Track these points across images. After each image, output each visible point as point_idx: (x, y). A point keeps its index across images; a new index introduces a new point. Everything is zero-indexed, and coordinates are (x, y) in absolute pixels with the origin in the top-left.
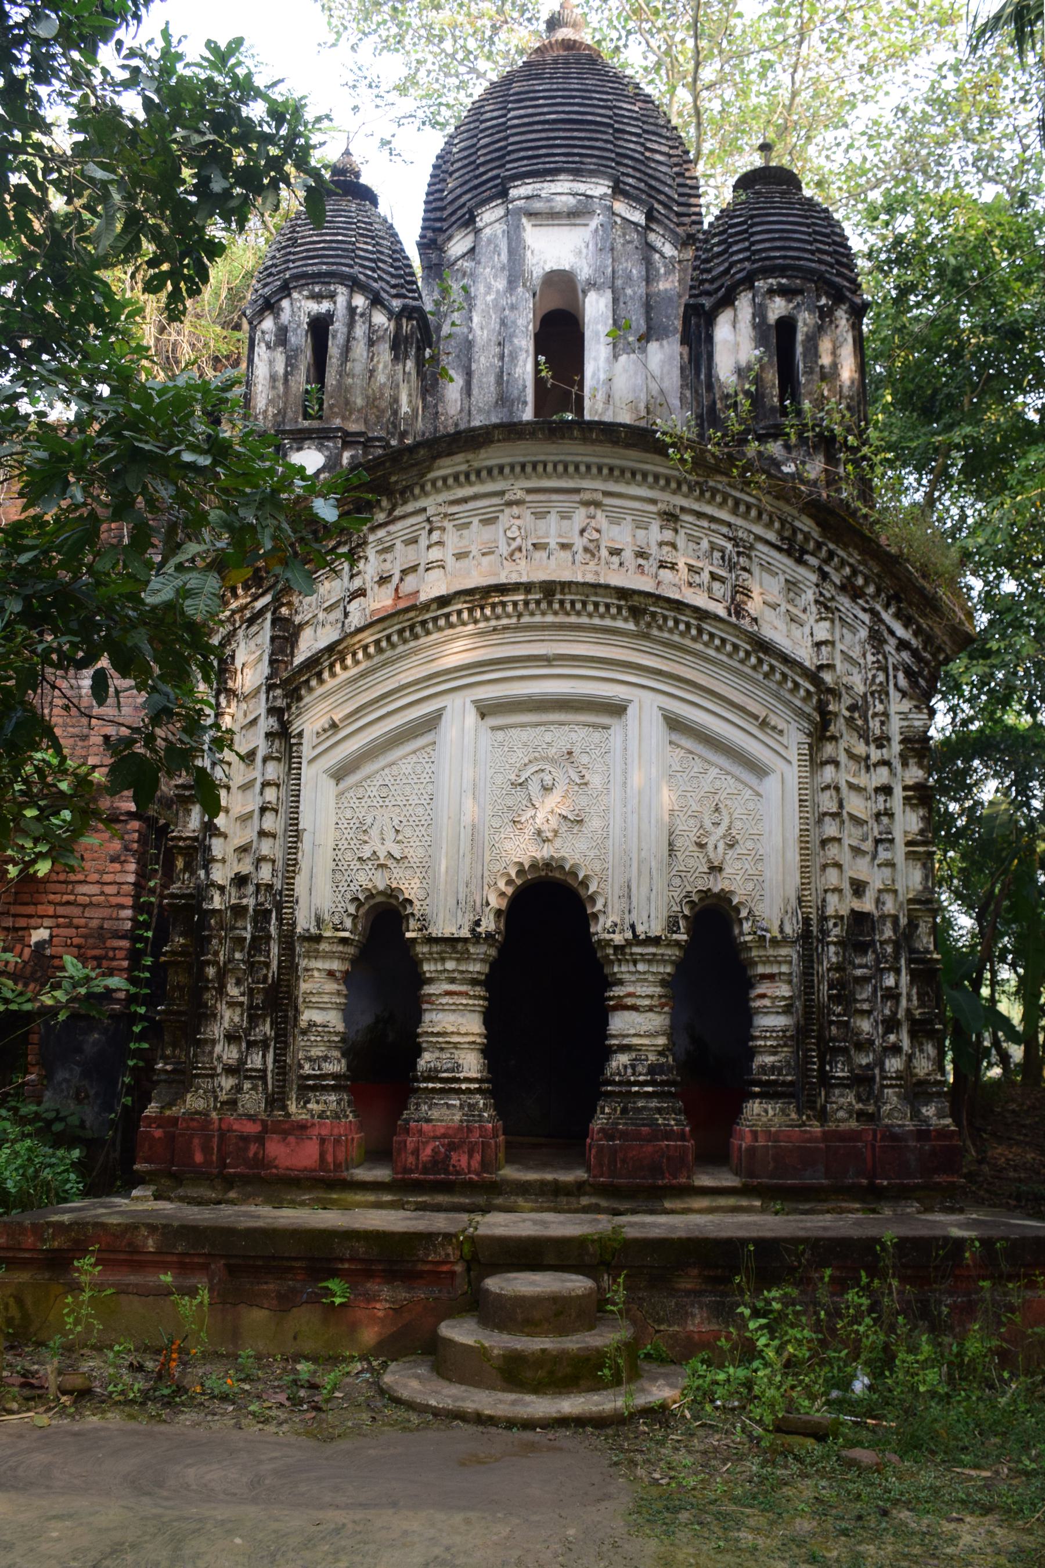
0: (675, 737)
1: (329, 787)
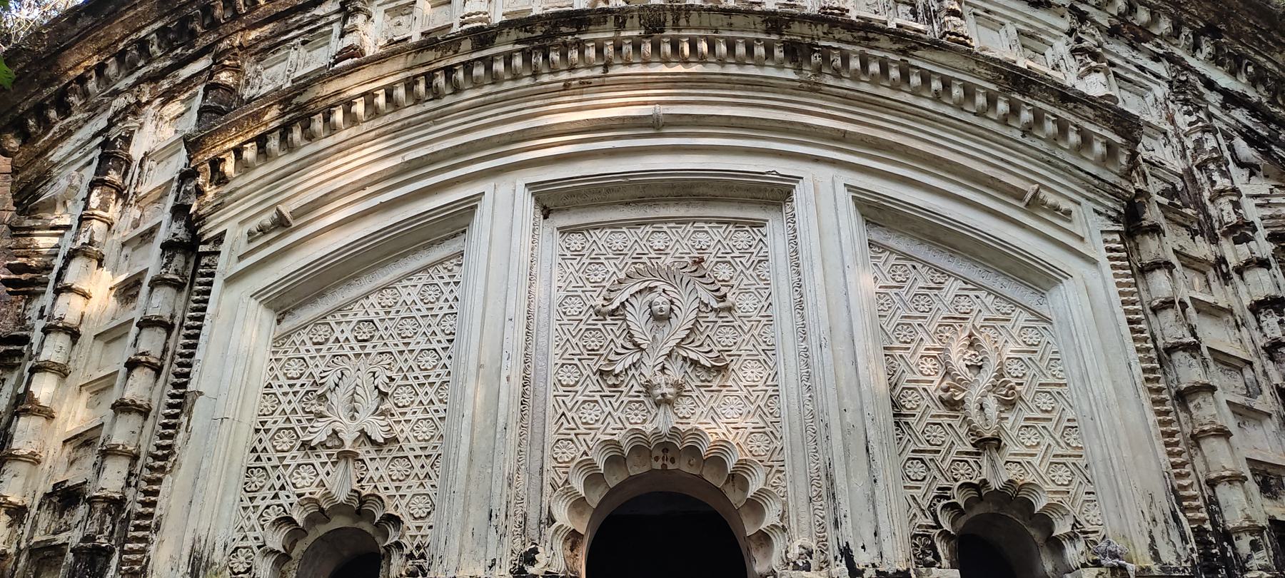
0: (877, 236)
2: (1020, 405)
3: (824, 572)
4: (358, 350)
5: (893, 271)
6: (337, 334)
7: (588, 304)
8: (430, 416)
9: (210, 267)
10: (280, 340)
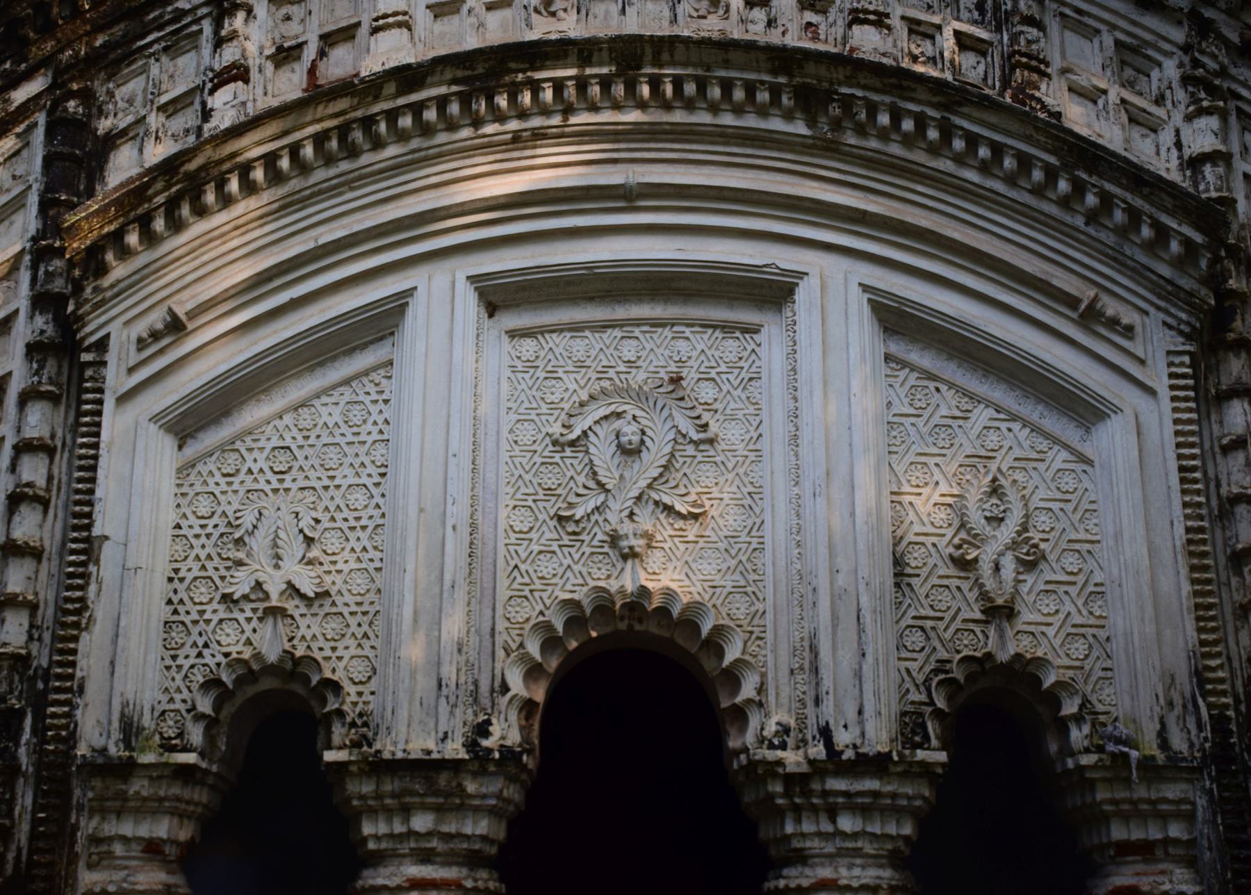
0: (895, 348)
1: (161, 453)
2: (1043, 565)
3: (801, 752)
4: (275, 485)
5: (911, 395)
6: (249, 464)
7: (544, 430)
8: (364, 565)
9: (96, 380)
10: (185, 470)
